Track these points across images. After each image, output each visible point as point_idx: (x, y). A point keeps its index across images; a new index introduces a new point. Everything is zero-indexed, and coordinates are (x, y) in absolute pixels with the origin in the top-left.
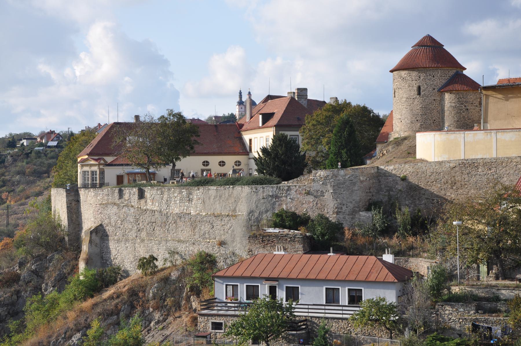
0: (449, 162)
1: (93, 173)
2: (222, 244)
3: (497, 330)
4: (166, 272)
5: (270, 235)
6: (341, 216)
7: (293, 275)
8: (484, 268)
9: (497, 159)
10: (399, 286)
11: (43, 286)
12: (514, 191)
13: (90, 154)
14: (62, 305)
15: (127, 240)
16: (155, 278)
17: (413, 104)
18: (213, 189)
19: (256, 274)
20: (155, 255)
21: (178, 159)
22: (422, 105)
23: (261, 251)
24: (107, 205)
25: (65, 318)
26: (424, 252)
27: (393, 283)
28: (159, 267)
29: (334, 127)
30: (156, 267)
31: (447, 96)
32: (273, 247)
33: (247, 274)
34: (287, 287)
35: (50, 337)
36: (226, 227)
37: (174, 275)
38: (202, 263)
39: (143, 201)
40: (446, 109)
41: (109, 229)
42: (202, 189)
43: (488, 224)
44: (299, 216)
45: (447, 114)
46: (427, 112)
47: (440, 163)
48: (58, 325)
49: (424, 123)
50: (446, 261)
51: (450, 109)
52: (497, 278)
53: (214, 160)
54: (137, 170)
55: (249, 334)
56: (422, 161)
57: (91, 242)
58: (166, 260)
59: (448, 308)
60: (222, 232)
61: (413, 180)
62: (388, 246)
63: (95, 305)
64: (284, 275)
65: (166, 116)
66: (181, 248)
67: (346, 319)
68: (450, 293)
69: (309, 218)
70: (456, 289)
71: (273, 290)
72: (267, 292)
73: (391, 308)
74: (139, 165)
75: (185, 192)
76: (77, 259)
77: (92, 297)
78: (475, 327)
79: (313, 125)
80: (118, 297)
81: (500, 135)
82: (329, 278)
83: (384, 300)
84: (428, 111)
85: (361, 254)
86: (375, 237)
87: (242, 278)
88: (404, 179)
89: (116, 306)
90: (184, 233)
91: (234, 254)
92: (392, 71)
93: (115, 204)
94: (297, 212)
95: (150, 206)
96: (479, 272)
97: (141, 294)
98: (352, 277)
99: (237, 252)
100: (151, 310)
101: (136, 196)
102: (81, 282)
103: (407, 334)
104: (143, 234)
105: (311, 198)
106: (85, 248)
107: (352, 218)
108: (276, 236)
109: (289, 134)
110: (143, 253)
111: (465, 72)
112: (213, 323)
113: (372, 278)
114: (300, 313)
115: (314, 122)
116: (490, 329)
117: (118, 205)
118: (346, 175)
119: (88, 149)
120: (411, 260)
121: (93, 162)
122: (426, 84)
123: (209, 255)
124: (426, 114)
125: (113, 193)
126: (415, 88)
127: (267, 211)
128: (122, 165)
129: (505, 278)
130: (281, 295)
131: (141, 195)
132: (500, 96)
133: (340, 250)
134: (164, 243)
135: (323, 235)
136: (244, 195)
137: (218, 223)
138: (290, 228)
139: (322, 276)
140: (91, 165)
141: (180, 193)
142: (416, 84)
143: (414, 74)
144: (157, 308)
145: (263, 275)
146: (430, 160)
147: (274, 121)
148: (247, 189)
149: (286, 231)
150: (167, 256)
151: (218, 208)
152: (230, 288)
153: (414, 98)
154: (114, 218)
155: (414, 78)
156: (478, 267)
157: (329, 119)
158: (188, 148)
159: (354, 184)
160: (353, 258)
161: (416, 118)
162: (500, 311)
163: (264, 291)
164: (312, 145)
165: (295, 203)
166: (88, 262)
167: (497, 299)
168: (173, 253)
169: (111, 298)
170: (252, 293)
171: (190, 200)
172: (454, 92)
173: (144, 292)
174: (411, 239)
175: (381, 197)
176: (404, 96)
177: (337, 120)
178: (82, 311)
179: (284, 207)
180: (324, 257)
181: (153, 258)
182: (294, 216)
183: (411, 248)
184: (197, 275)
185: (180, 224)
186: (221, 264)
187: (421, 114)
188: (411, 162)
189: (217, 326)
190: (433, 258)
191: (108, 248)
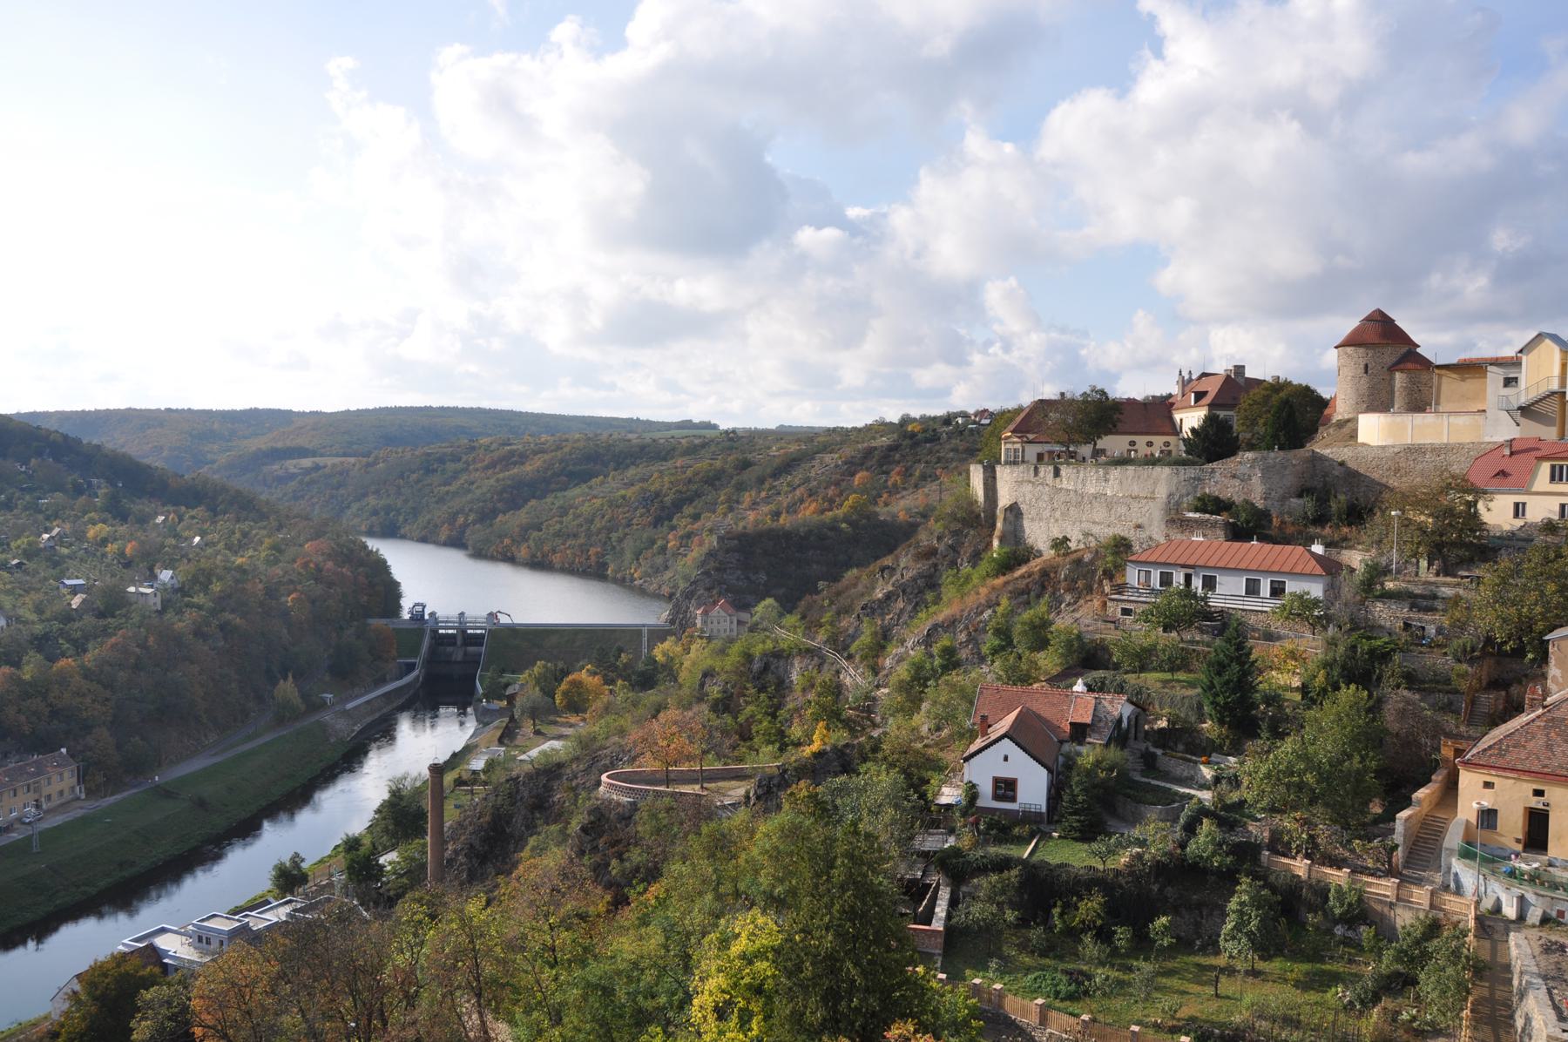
0: (1393, 447)
1: (1015, 450)
2: (1139, 526)
3: (1431, 630)
4: (1079, 554)
5: (1189, 520)
6: (1269, 502)
7: (1211, 564)
8: (1424, 563)
9: (1446, 445)
10: (1328, 579)
11: (959, 560)
12: (1463, 480)
13: (1012, 432)
14: (975, 581)
15: (1041, 519)
16: (1068, 559)
18: (1131, 468)
19: (1171, 561)
20: (1069, 536)
21: (1099, 437)
23: (1179, 536)
24: (1022, 482)
25: (978, 594)
26: (1359, 544)
27: (1321, 575)
28: (1073, 549)
29: (1271, 407)
30: (1069, 548)
31: (1398, 375)
32: (1192, 532)
33: (1162, 560)
34: (1204, 576)
35: (962, 611)
36: (1144, 510)
37: (1087, 557)
38: (1116, 546)
39: (1058, 480)
40: (1396, 389)
41: (1023, 507)
42: (1119, 468)
43: (1429, 516)
44: (1223, 501)
45: (1397, 394)
47: (1383, 448)
48: (971, 600)
50: (1382, 554)
51: (1401, 390)
52: (1437, 575)
53: (1141, 440)
54: (1057, 448)
55: (1159, 622)
56: (1364, 445)
57: (1005, 519)
58: (1079, 541)
59: (1378, 604)
60: (1139, 515)
61: (1352, 465)
62: (1318, 536)
63: (1007, 583)
64: (1200, 563)
65: (1088, 392)
66: (1096, 530)
67: (1266, 612)
68: (1384, 589)
69: (1234, 503)
70: (1390, 585)
71: (1188, 578)
72: (1182, 581)
73: (1316, 603)
74: (1058, 442)
75: (1101, 471)
76: (991, 536)
77: (1004, 574)
78: (1407, 626)
79: (1250, 405)
80: (1029, 576)
81: (1452, 419)
82: (1230, 566)
83: (1308, 593)
85: (1288, 544)
86: (1305, 526)
87: (1156, 564)
88: (1342, 464)
89: (1027, 585)
90: (1099, 514)
91: (1150, 538)
92: (1336, 347)
93: (1030, 482)
94: (1221, 496)
95: (1065, 484)
96: (1418, 568)
97: (1052, 575)
98: (1275, 568)
99: (1155, 536)
100: (1062, 591)
101: (1051, 475)
102: (994, 560)
103: (1331, 631)
104: (1058, 514)
105: (1237, 482)
106: (999, 525)
107: (1282, 505)
108: (1196, 521)
109: (1222, 414)
110: (1057, 533)
111: (1418, 350)
112: (1123, 609)
113: (1298, 570)
114: (1215, 602)
115: (1251, 402)
116: (1423, 628)
117: (1033, 483)
118: (1276, 458)
119: (1012, 427)
120: (1344, 552)
121: (1016, 440)
123: (1124, 539)
125: (1028, 470)
126: (1362, 366)
127: (1188, 495)
128: (1042, 442)
129: (1446, 575)
130: (1197, 583)
131: (1057, 473)
132: (1454, 376)
133: (1264, 538)
134: (1078, 524)
135: (1248, 522)
136: (1164, 476)
137: (1135, 505)
138: (1212, 513)
139: (1242, 566)
140: (1014, 443)
141: (1097, 472)
144: (1068, 590)
145: (1178, 562)
146: (1372, 444)
147: (1208, 399)
148: (1167, 470)
149: (1207, 516)
150: (1081, 537)
151: (1135, 490)
152: (1143, 574)
154: (1029, 496)
156: (1418, 562)
157: (1267, 398)
158: (1111, 426)
159: (1285, 468)
160: (1278, 547)
162: (1436, 610)
163: (1178, 578)
164: (1248, 427)
165: (1219, 486)
166: (1002, 540)
167: (1434, 597)
168: (1087, 534)
169: (1022, 577)
170: (1166, 580)
171: (1107, 480)
173: (1056, 572)
174: (1345, 530)
175: (1316, 483)
177: (1275, 399)
178: (993, 588)
179: (1207, 491)
180: (1247, 545)
181: (1066, 539)
182: (1217, 499)
183: (1345, 539)
184: (1109, 558)
185: (1096, 504)
186: (1136, 548)
188: (1351, 445)
189: (1126, 612)
190: (1367, 551)
191: (1022, 526)
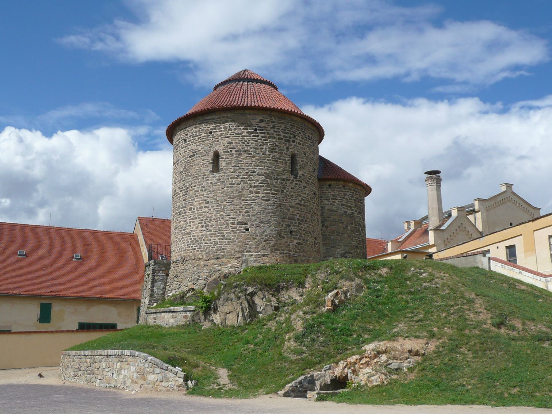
17: (282, 192)
22: (300, 198)
46: (308, 218)
49: (304, 240)
84: (309, 216)
122: (305, 154)
124: (306, 221)
126: (287, 158)
142: (288, 149)
143: (283, 126)
153: (283, 180)
155: (282, 134)
161: (288, 226)
172: (351, 185)
176: (257, 170)
187: (298, 219)
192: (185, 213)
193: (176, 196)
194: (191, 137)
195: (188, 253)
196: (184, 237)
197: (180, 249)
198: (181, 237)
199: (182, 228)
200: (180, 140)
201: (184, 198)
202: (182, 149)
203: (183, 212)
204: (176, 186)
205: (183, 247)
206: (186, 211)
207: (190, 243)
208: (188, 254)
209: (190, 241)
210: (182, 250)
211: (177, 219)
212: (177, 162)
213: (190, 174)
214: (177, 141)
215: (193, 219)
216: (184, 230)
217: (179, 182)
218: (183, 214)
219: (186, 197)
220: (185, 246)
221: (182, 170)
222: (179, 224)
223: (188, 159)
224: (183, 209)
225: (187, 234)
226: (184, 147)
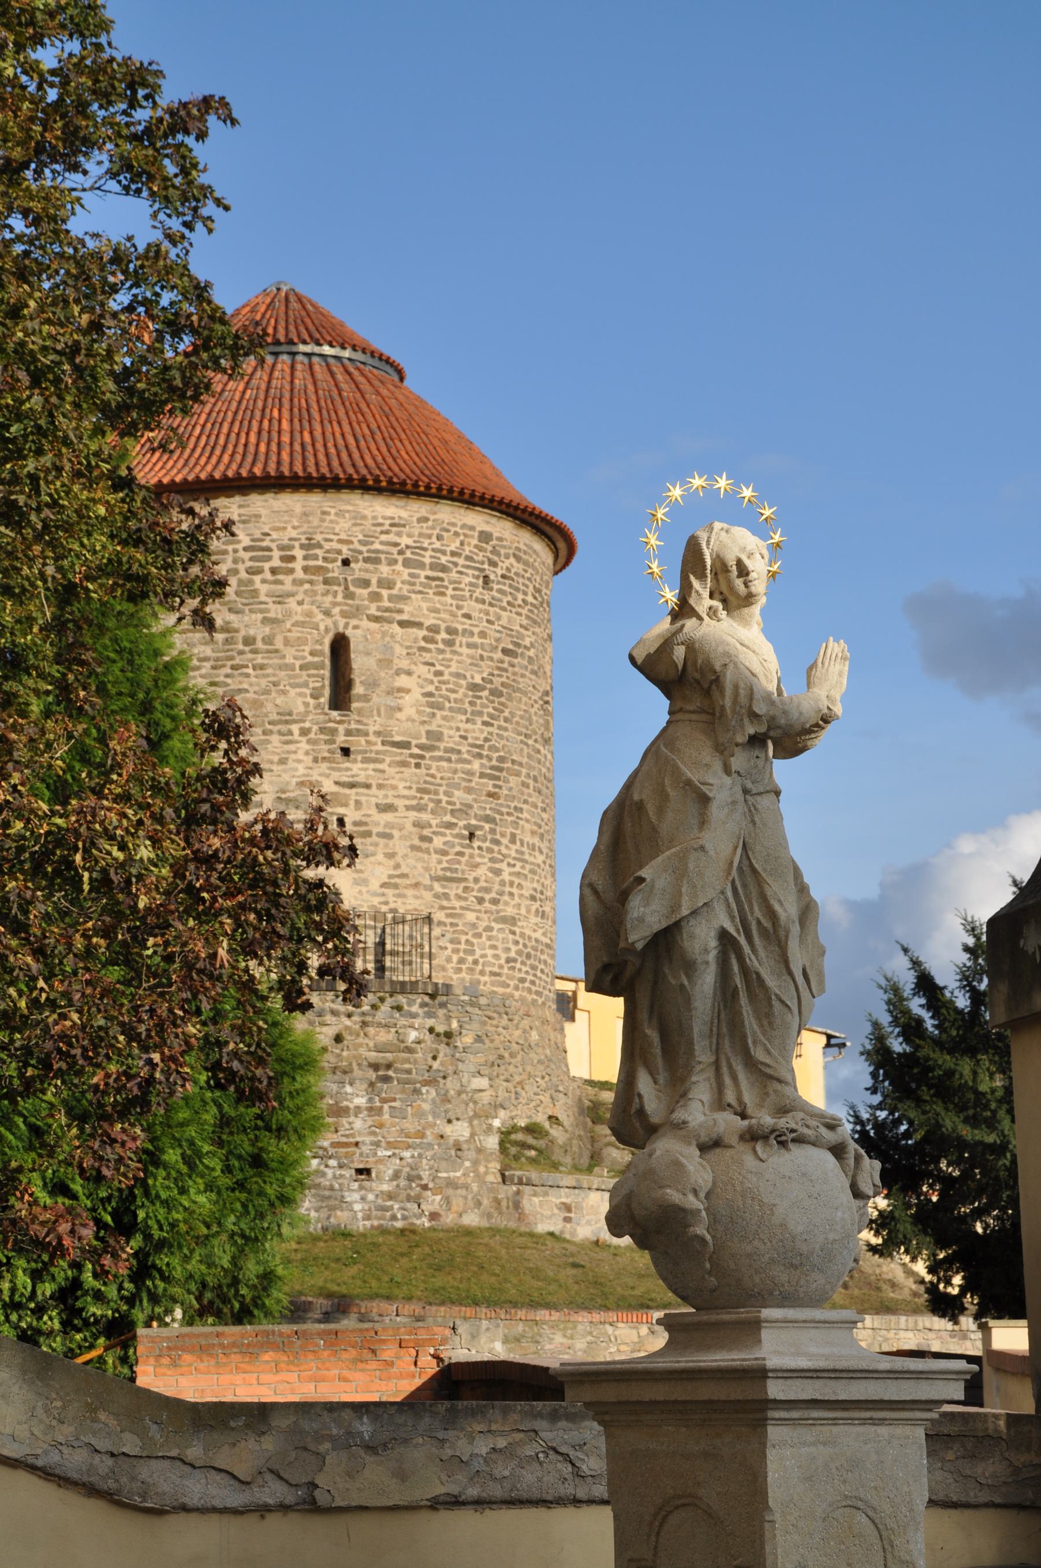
192: (497, 842)
193: (449, 760)
194: (507, 582)
195: (508, 986)
196: (496, 926)
197: (476, 962)
198: (485, 924)
199: (487, 890)
200: (461, 561)
201: (491, 789)
202: (473, 603)
203: (489, 837)
204: (438, 720)
205: (490, 959)
206: (498, 837)
207: (513, 954)
208: (508, 990)
209: (514, 948)
210: (488, 969)
211: (458, 849)
212: (444, 635)
213: (506, 714)
214: (444, 553)
215: (518, 874)
216: (495, 902)
217: (464, 718)
218: (488, 844)
219: (500, 787)
220: (496, 957)
221: (478, 680)
222: (474, 874)
223: (499, 655)
224: (487, 826)
225: (504, 920)
226: (483, 602)
